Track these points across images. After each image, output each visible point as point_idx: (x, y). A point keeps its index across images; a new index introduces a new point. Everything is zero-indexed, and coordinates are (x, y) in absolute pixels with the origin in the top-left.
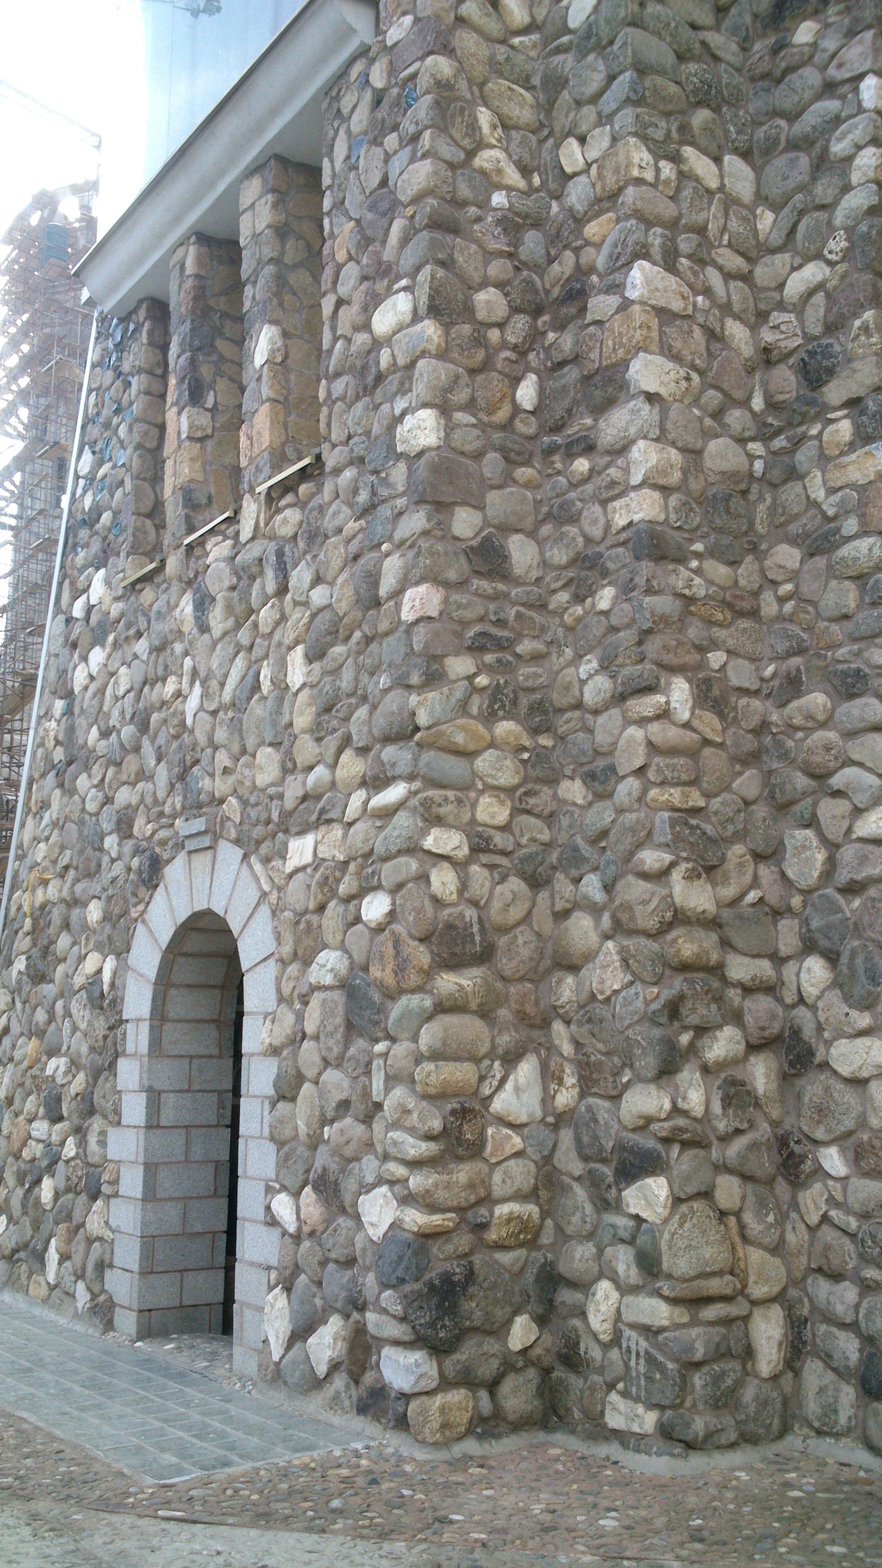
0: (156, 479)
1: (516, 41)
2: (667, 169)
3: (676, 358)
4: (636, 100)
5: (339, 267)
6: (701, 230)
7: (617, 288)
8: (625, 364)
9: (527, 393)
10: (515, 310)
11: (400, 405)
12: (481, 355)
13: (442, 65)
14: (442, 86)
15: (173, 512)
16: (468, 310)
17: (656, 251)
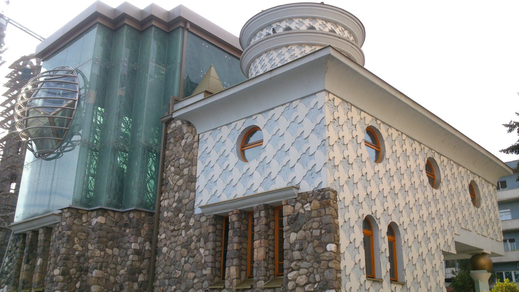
0: (18, 277)
1: (84, 224)
2: (102, 253)
3: (100, 285)
4: (98, 242)
5: (51, 258)
6: (108, 262)
7: (92, 273)
8: (91, 286)
9: (78, 285)
10: (77, 271)
11: (56, 288)
12: (70, 280)
13: (69, 233)
14: (69, 236)
15: (21, 284)
16: (69, 273)
17: (98, 268)
